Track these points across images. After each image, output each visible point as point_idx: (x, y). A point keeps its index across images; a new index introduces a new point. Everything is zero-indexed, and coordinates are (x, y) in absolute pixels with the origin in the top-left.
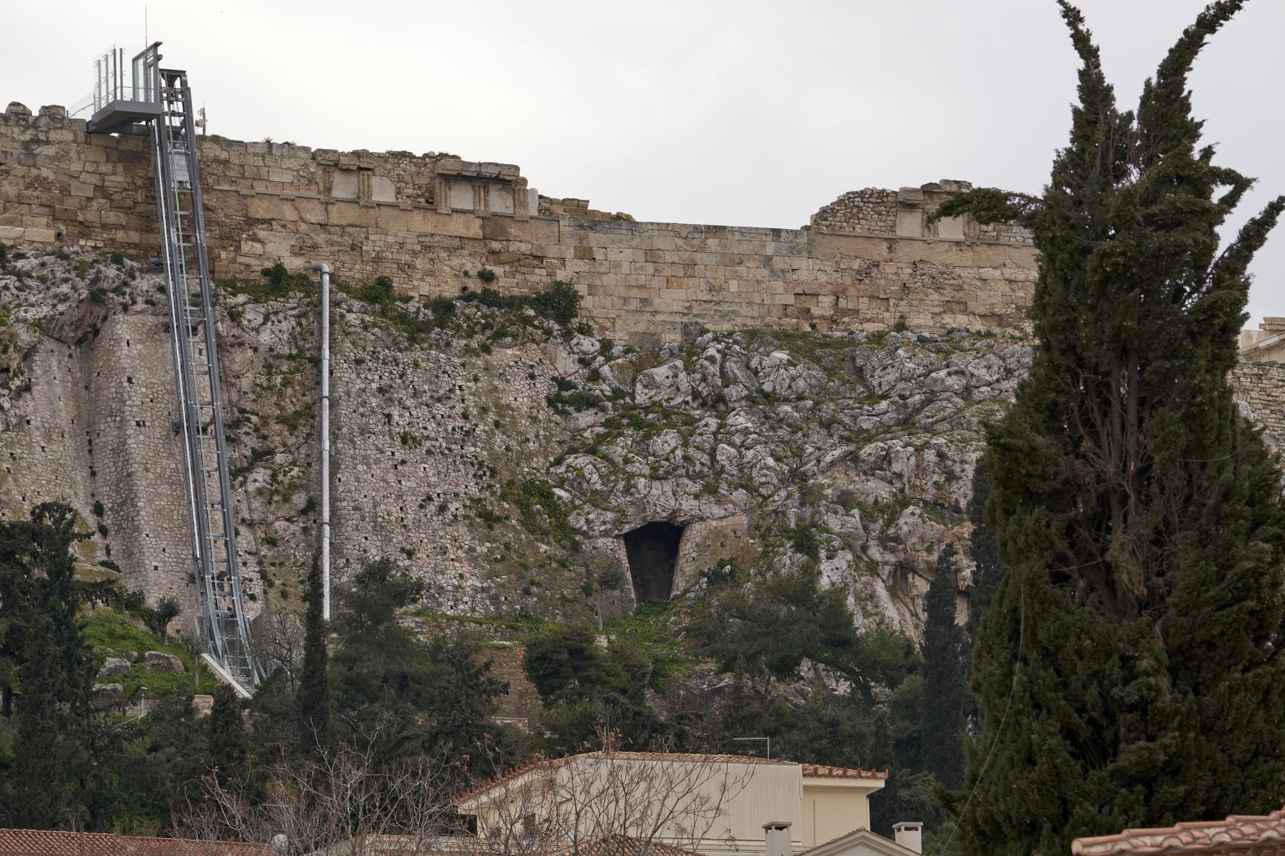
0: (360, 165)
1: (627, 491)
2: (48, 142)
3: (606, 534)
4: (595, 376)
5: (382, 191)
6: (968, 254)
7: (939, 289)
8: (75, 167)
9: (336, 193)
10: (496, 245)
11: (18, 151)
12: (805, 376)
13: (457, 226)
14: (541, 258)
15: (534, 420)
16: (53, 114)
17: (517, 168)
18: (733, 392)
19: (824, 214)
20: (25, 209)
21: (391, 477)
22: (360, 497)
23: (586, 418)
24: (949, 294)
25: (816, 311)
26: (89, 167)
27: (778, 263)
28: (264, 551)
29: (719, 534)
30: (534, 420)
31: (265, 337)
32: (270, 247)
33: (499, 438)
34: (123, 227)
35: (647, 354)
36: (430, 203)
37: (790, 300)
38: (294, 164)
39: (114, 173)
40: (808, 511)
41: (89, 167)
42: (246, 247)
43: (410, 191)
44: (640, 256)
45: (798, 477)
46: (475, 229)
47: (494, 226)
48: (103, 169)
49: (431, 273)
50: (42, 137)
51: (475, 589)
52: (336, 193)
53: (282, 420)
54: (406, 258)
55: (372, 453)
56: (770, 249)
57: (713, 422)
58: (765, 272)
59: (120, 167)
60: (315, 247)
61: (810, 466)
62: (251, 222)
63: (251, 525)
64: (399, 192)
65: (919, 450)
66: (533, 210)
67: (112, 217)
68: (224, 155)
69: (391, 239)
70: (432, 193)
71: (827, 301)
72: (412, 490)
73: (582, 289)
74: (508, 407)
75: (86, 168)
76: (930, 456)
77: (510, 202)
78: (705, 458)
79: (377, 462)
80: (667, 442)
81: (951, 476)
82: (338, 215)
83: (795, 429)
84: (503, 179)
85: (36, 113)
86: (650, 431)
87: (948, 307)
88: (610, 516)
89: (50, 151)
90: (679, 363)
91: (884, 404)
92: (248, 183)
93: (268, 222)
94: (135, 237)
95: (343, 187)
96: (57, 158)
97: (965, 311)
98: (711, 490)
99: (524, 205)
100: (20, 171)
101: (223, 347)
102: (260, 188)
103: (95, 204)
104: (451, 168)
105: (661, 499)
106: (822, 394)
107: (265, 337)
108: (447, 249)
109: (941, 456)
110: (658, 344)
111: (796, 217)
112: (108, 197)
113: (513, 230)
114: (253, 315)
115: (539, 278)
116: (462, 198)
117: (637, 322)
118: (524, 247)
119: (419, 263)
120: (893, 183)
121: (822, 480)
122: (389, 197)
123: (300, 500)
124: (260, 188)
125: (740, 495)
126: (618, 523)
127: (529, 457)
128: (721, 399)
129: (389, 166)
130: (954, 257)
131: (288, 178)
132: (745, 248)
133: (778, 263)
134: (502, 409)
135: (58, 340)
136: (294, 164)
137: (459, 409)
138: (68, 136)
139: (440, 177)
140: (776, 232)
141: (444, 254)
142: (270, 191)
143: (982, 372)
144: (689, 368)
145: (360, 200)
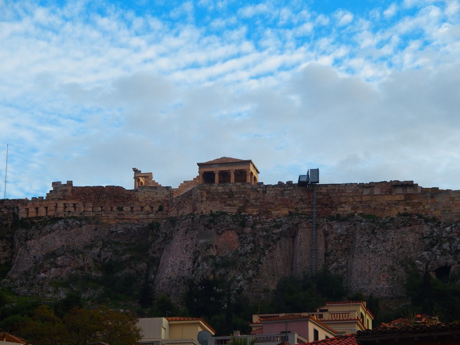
0: (371, 186)
2: (287, 190)
5: (377, 191)
8: (295, 195)
9: (364, 194)
10: (409, 201)
13: (397, 198)
14: (421, 203)
16: (290, 183)
17: (413, 181)
20: (281, 206)
21: (368, 262)
22: (357, 267)
26: (298, 195)
31: (339, 231)
32: (345, 209)
34: (306, 208)
36: (390, 193)
38: (353, 188)
39: (305, 195)
41: (298, 195)
42: (339, 209)
43: (384, 191)
47: (408, 197)
48: (302, 195)
50: (286, 189)
51: (387, 288)
52: (364, 194)
54: (382, 207)
59: (306, 194)
60: (358, 207)
62: (341, 203)
64: (381, 191)
67: (304, 206)
68: (334, 188)
69: (378, 203)
70: (391, 191)
72: (373, 265)
74: (406, 241)
77: (413, 190)
79: (364, 258)
82: (364, 199)
84: (409, 185)
85: (285, 183)
89: (288, 192)
92: (340, 194)
93: (345, 202)
94: (309, 210)
95: (366, 192)
96: (290, 193)
99: (416, 190)
100: (280, 198)
101: (326, 234)
102: (343, 194)
103: (299, 203)
105: (442, 261)
107: (339, 231)
108: (394, 204)
114: (336, 226)
117: (447, 216)
118: (416, 201)
119: (387, 208)
124: (343, 194)
129: (379, 185)
131: (351, 191)
134: (403, 242)
135: (285, 237)
136: (353, 188)
141: (394, 205)
142: (346, 195)
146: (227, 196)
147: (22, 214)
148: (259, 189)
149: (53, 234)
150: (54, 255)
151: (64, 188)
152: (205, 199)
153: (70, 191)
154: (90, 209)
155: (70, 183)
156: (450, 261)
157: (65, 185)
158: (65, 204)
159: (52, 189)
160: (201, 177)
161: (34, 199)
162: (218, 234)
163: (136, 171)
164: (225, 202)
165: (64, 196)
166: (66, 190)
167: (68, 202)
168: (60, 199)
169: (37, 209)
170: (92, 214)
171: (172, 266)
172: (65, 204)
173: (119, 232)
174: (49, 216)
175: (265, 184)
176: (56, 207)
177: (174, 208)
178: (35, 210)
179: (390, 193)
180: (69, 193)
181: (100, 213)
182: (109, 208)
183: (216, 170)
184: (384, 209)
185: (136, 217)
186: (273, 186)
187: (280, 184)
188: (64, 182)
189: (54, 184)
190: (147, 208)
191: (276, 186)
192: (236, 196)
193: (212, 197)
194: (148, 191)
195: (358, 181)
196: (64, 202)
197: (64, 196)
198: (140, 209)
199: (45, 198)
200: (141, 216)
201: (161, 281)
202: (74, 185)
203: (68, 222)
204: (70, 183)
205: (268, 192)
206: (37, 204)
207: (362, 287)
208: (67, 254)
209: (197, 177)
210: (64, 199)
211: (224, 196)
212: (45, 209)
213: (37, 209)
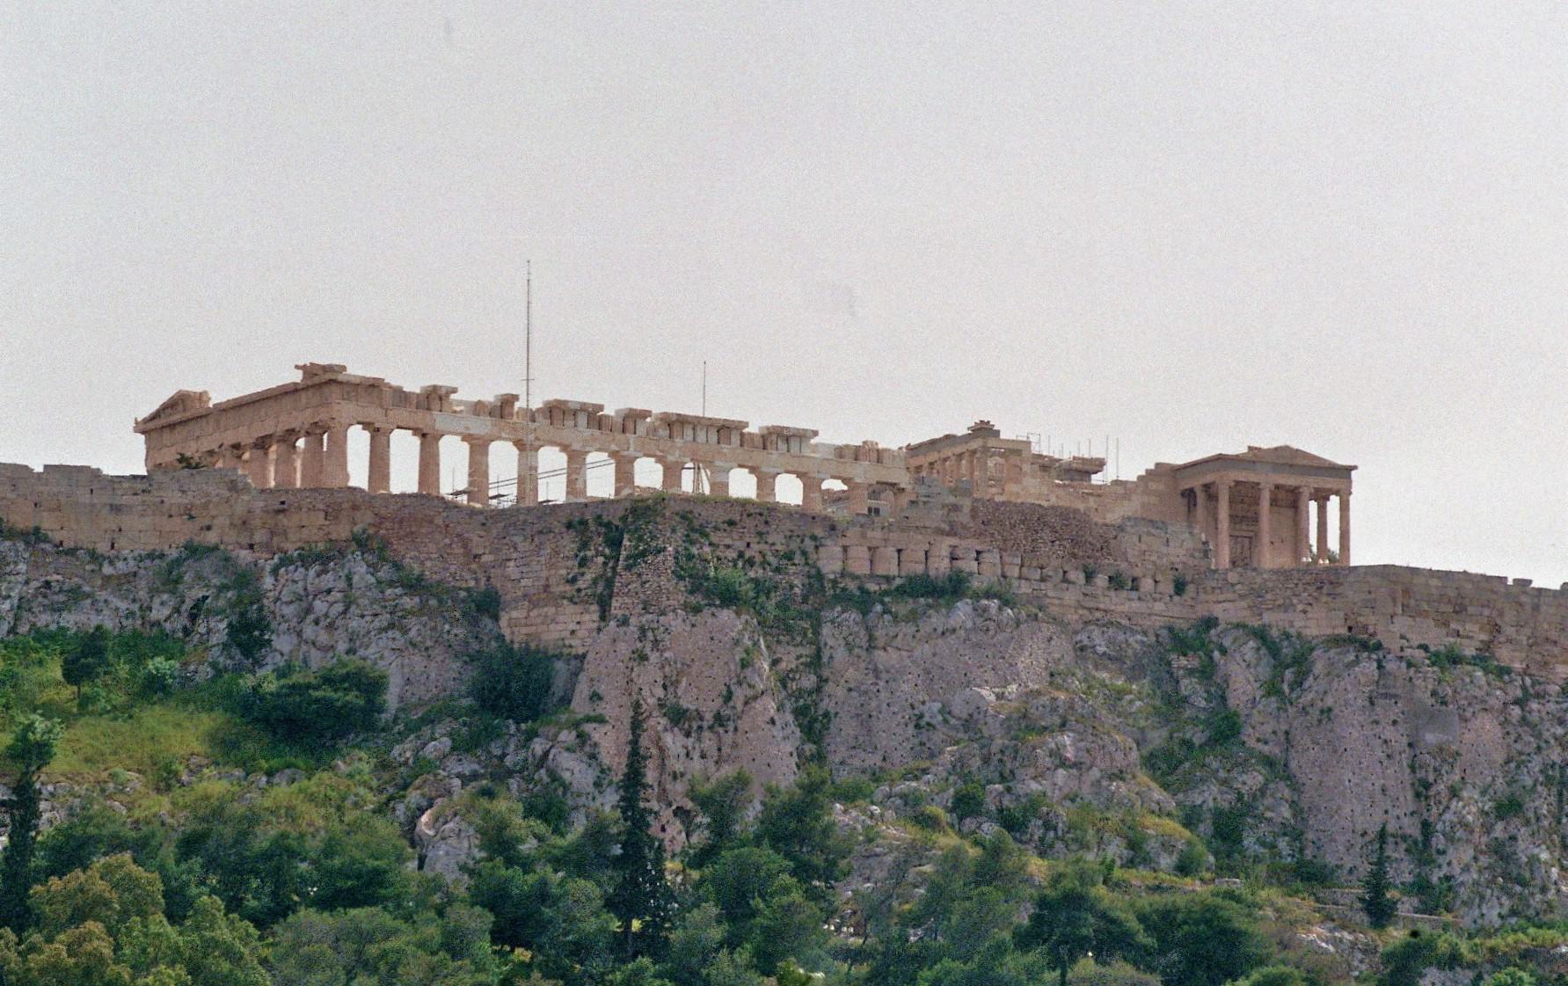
148: (1524, 599)
149: (951, 639)
153: (966, 510)
164: (1446, 624)
166: (955, 508)
167: (964, 543)
168: (940, 532)
177: (1230, 596)
180: (964, 517)
181: (1043, 586)
183: (1267, 480)
192: (1471, 610)
194: (1149, 534)
197: (952, 524)
203: (986, 609)
209: (1149, 472)
210: (952, 533)
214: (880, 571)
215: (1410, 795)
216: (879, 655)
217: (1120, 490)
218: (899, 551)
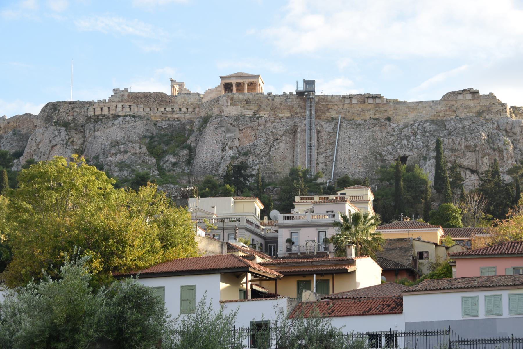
0: (350, 97)
1: (396, 151)
3: (392, 160)
4: (395, 131)
6: (472, 101)
7: (466, 109)
8: (295, 102)
11: (284, 101)
12: (432, 127)
13: (370, 106)
15: (381, 140)
16: (291, 94)
18: (418, 131)
19: (443, 97)
23: (392, 139)
24: (468, 110)
25: (441, 115)
27: (433, 107)
28: (324, 168)
29: (412, 158)
30: (381, 140)
31: (327, 129)
33: (372, 144)
35: (406, 126)
37: (435, 113)
40: (427, 152)
44: (405, 108)
45: (427, 146)
46: (373, 106)
49: (364, 115)
53: (330, 144)
55: (345, 148)
56: (431, 104)
57: (413, 138)
58: (430, 109)
61: (429, 144)
63: (322, 163)
65: (449, 139)
66: (385, 102)
67: (302, 111)
71: (443, 113)
72: (352, 155)
73: (394, 115)
75: (296, 102)
76: (451, 140)
78: (411, 144)
80: (405, 142)
81: (454, 143)
83: (428, 137)
84: (378, 97)
86: (402, 140)
87: (468, 112)
88: (392, 156)
89: (290, 100)
90: (410, 127)
91: (445, 131)
97: (472, 112)
98: (411, 150)
104: (367, 96)
105: (402, 153)
106: (436, 130)
109: (453, 140)
110: (409, 124)
111: (438, 98)
112: (301, 107)
113: (381, 106)
115: (386, 115)
116: (371, 101)
120: (457, 90)
121: (431, 146)
122: (356, 102)
123: (331, 158)
125: (416, 150)
126: (394, 158)
127: (379, 147)
128: (417, 133)
130: (469, 102)
132: (427, 105)
133: (433, 107)
137: (364, 139)
138: (293, 97)
139: (365, 98)
140: (433, 101)
143: (467, 124)
144: (411, 128)
145: (351, 103)
146: (245, 102)
147: (91, 113)
148: (269, 98)
149: (115, 127)
150: (117, 143)
151: (122, 93)
152: (229, 104)
153: (126, 95)
154: (142, 110)
155: (126, 90)
156: (408, 153)
157: (123, 91)
158: (123, 105)
159: (113, 94)
160: (223, 86)
161: (100, 102)
162: (240, 130)
163: (172, 80)
165: (122, 99)
166: (123, 95)
167: (125, 104)
168: (119, 102)
169: (102, 109)
170: (143, 113)
171: (206, 153)
172: (123, 105)
173: (164, 127)
174: (112, 114)
175: (274, 94)
176: (116, 107)
178: (100, 110)
179: (364, 102)
180: (126, 97)
182: (156, 109)
183: (234, 81)
184: (360, 114)
185: (176, 116)
186: (279, 96)
187: (285, 94)
188: (122, 89)
189: (114, 90)
190: (184, 110)
191: (282, 95)
192: (252, 102)
193: (234, 102)
195: (341, 94)
196: (122, 104)
197: (122, 99)
198: (178, 110)
199: (107, 101)
200: (180, 115)
201: (198, 164)
202: (129, 91)
204: (126, 90)
205: (275, 100)
206: (102, 105)
207: (344, 170)
208: (127, 143)
209: (218, 86)
210: (122, 102)
211: (243, 102)
212: (107, 109)
213: (102, 109)
214: (103, 113)
215: (220, 151)
216: (97, 134)
217: (210, 91)
218: (109, 108)
